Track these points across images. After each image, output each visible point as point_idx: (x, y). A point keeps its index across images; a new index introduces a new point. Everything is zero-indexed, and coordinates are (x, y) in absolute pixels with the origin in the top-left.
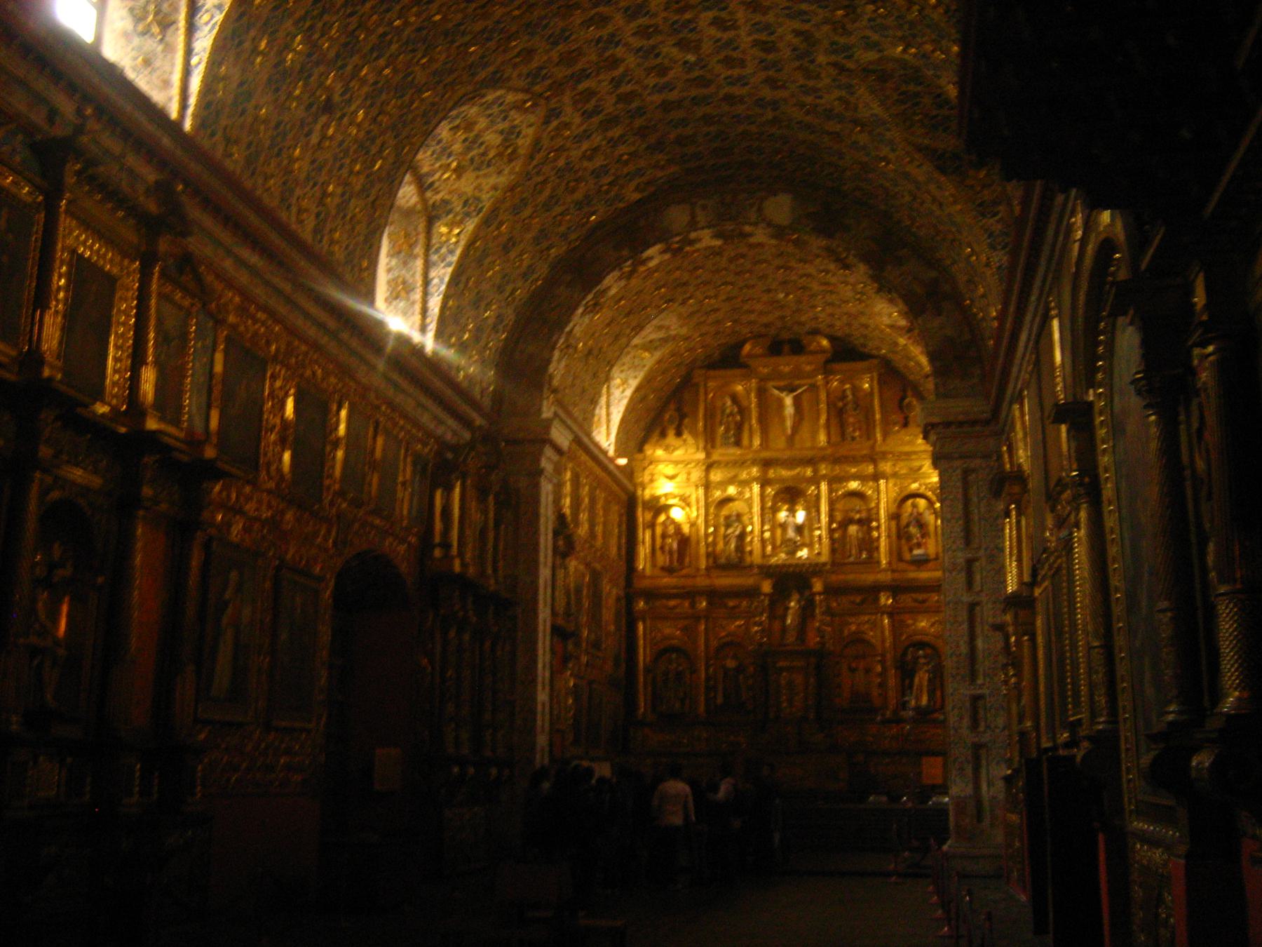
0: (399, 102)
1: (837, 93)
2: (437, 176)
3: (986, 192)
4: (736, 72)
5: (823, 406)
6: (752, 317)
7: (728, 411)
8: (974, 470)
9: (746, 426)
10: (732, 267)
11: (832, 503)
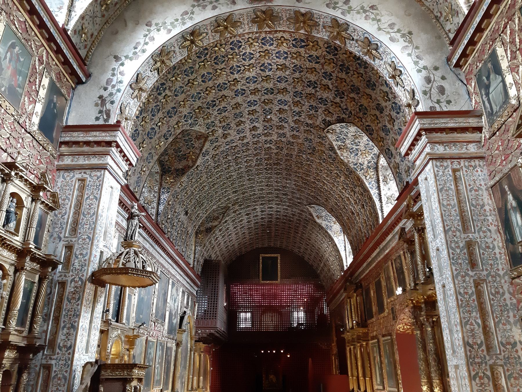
4: (253, 108)
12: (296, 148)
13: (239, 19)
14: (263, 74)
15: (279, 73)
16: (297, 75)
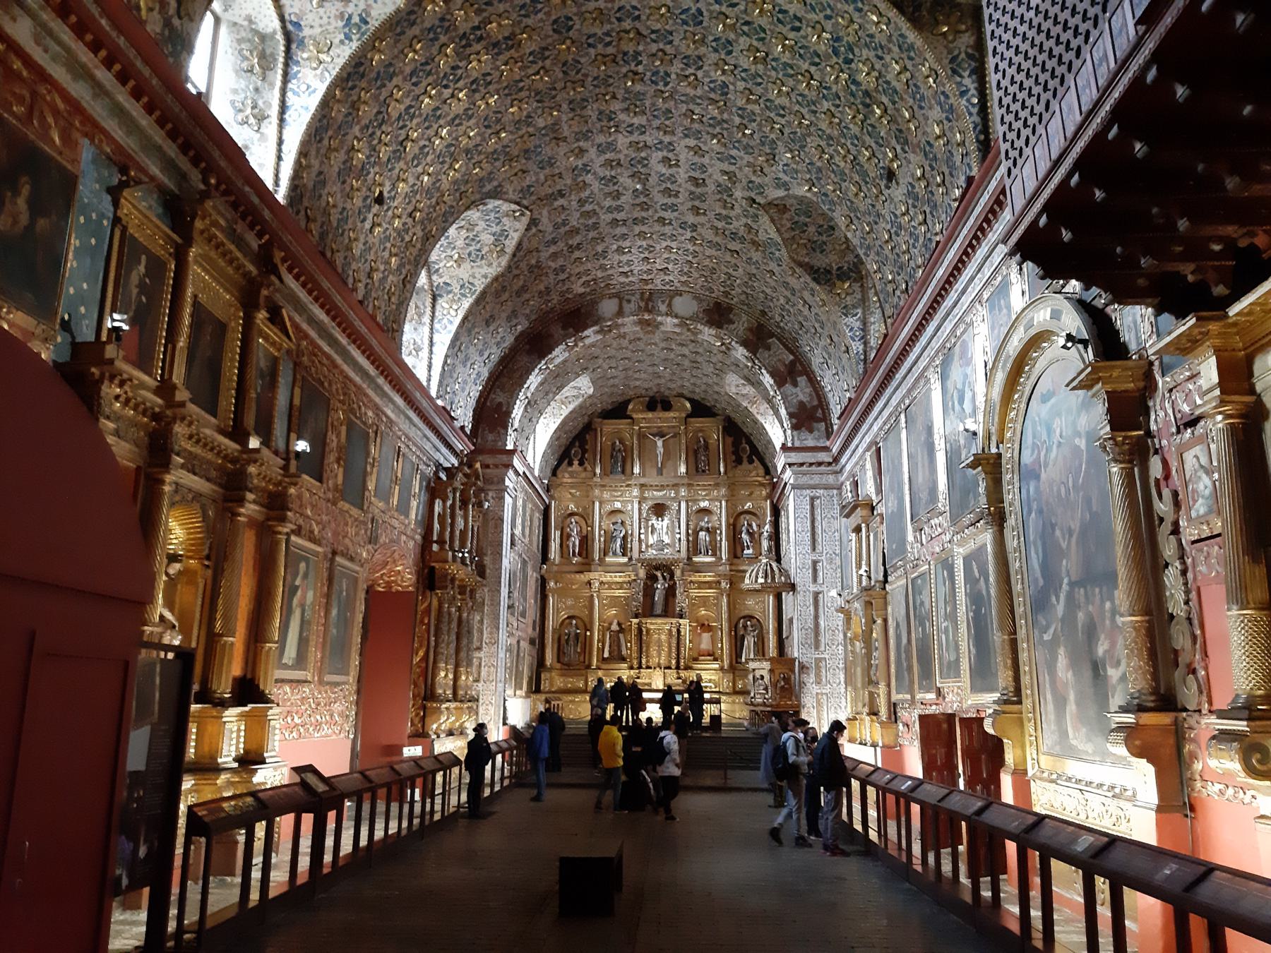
0: (428, 202)
1: (744, 220)
2: (441, 265)
3: (848, 298)
4: (670, 201)
5: (684, 447)
6: (638, 383)
7: (617, 449)
8: (818, 498)
10: (630, 347)
11: (688, 515)
12: (566, 133)
14: (651, 242)
15: (627, 243)
16: (600, 249)
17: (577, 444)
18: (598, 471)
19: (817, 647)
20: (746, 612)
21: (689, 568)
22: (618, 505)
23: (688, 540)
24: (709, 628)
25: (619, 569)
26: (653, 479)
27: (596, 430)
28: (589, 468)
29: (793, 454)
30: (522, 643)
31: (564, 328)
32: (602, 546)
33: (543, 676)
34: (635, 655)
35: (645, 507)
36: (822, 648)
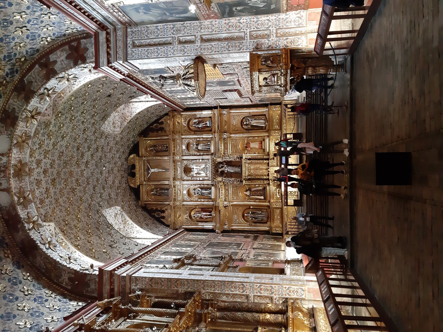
5: (155, 158)
6: (117, 182)
9: (162, 186)
13: (24, 152)
17: (153, 214)
18: (167, 203)
19: (242, 38)
20: (239, 124)
21: (217, 154)
22: (185, 192)
23: (203, 155)
24: (248, 143)
25: (218, 191)
26: (171, 174)
27: (145, 204)
28: (166, 208)
29: (101, 60)
30: (255, 246)
31: (18, 231)
32: (206, 200)
33: (274, 232)
34: (262, 182)
35: (186, 178)
36: (243, 34)
